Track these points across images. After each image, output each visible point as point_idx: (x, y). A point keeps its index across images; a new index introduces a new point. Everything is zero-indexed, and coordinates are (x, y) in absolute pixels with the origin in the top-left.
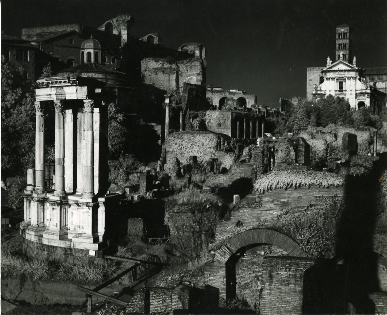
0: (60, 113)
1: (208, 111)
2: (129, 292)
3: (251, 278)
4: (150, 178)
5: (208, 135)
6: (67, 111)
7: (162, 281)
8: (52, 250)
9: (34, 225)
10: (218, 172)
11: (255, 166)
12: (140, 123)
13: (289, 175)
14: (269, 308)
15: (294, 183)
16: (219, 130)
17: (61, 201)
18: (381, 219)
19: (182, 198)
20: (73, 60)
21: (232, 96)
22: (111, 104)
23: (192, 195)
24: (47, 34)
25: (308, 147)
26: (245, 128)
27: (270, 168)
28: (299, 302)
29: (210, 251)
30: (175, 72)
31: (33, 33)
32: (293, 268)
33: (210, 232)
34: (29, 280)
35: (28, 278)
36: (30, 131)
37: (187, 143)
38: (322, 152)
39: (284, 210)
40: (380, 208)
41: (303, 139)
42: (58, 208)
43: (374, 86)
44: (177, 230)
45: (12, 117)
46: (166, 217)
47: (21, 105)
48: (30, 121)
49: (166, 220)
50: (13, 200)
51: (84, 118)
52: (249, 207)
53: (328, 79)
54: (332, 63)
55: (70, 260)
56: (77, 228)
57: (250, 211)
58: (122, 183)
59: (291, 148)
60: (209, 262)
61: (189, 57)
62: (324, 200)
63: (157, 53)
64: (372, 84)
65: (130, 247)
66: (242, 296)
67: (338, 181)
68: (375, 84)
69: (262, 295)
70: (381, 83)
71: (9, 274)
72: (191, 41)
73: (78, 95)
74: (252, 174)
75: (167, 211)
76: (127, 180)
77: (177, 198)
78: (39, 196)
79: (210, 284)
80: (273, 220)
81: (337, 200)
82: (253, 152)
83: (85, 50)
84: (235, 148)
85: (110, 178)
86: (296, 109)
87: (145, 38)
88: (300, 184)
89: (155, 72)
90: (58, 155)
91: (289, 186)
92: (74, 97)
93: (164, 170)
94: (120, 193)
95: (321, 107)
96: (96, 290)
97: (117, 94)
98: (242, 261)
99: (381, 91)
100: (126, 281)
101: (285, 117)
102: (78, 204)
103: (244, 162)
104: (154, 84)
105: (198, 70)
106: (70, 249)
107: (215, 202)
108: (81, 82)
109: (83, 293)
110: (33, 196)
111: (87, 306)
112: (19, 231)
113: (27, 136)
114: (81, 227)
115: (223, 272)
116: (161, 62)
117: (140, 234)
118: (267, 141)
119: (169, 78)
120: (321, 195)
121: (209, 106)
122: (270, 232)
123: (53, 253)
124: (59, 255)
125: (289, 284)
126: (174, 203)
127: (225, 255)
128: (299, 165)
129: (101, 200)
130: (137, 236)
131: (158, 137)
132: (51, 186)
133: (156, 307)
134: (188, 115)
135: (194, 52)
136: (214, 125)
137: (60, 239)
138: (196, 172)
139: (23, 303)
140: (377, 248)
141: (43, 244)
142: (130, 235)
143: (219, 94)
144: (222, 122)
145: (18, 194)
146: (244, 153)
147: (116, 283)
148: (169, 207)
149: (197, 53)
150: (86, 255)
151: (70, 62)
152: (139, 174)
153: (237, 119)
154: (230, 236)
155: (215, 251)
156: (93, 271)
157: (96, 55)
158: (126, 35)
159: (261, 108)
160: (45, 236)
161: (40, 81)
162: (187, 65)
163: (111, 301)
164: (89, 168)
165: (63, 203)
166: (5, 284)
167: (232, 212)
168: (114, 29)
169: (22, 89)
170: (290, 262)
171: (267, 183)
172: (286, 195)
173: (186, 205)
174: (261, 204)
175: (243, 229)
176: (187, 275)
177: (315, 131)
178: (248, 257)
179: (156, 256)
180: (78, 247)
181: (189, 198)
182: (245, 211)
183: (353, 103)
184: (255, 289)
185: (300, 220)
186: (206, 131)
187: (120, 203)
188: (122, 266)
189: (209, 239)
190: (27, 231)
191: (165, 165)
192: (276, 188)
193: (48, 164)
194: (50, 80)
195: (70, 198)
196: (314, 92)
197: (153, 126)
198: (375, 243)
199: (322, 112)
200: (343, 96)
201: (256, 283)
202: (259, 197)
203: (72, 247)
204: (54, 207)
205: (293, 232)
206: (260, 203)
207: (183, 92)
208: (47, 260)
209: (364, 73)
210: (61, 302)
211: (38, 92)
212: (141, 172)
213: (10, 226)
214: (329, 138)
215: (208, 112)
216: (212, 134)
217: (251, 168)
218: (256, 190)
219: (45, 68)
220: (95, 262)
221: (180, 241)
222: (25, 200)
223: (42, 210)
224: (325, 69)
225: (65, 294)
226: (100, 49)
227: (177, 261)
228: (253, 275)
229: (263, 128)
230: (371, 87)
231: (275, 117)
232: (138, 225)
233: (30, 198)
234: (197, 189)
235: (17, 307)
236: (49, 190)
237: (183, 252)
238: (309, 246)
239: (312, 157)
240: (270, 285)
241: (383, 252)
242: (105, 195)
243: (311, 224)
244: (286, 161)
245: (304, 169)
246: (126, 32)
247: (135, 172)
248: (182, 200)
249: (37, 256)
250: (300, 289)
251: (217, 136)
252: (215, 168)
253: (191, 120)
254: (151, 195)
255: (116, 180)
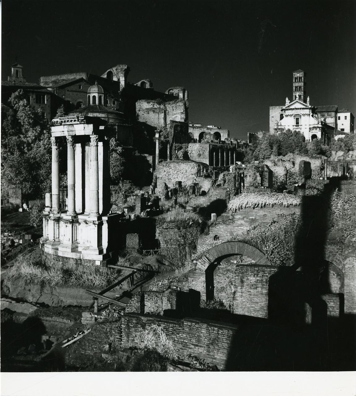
0: (72, 147)
1: (190, 144)
2: (127, 295)
3: (227, 283)
4: (144, 200)
5: (190, 163)
6: (77, 145)
7: (154, 285)
8: (66, 261)
9: (51, 240)
10: (198, 194)
11: (228, 189)
12: (136, 154)
13: (256, 196)
14: (241, 308)
15: (260, 203)
16: (199, 159)
17: (73, 220)
18: (331, 232)
19: (169, 216)
20: (81, 102)
21: (209, 131)
22: (112, 138)
23: (178, 214)
24: (60, 81)
25: (271, 173)
26: (221, 158)
27: (241, 190)
28: (265, 302)
29: (193, 260)
30: (163, 111)
31: (49, 80)
32: (260, 274)
33: (193, 244)
34: (47, 285)
35: (47, 284)
36: (47, 162)
37: (173, 171)
38: (282, 177)
39: (253, 226)
40: (330, 223)
41: (267, 166)
42: (70, 226)
43: (324, 121)
44: (166, 244)
45: (33, 150)
46: (157, 232)
47: (40, 140)
48: (48, 154)
49: (157, 235)
50: (34, 219)
51: (91, 150)
52: (224, 223)
53: (287, 116)
54: (290, 103)
55: (80, 269)
56: (85, 242)
57: (225, 227)
58: (121, 205)
59: (258, 174)
60: (192, 269)
61: (174, 98)
62: (285, 217)
63: (149, 96)
64: (322, 119)
65: (128, 258)
66: (219, 298)
67: (296, 201)
68: (325, 120)
69: (235, 297)
70: (330, 119)
71: (32, 281)
72: (176, 85)
73: (86, 131)
74: (226, 196)
75: (158, 228)
76: (126, 202)
77: (166, 217)
78: (55, 216)
79: (193, 288)
80: (244, 234)
81: (295, 217)
82: (227, 178)
83: (91, 94)
84: (212, 174)
85: (112, 200)
86: (261, 142)
87: (139, 84)
88: (265, 204)
89: (147, 112)
90: (70, 182)
91: (256, 206)
92: (82, 133)
93: (155, 193)
94: (120, 213)
95: (281, 139)
96: (101, 294)
97: (117, 130)
98: (219, 269)
99: (330, 125)
100: (125, 286)
101: (252, 148)
102: (86, 222)
103: (219, 185)
104: (147, 122)
105: (182, 109)
106: (80, 260)
107: (196, 219)
108: (88, 121)
109: (91, 296)
110: (50, 216)
111: (94, 307)
112: (39, 245)
113: (45, 166)
114: (89, 241)
115: (203, 278)
116: (152, 103)
117: (136, 247)
118: (238, 168)
119: (159, 116)
120: (282, 213)
121: (191, 140)
122: (241, 244)
123: (67, 263)
124: (71, 265)
125: (257, 288)
126: (163, 221)
127: (205, 263)
128: (264, 188)
129: (105, 219)
130: (134, 248)
131: (150, 166)
132: (64, 207)
133: (149, 308)
134: (174, 147)
135: (178, 94)
136: (195, 155)
137: (72, 252)
138: (181, 194)
139: (43, 305)
140: (329, 257)
141: (59, 256)
142: (128, 248)
143: (199, 129)
144: (201, 153)
145: (38, 215)
146: (220, 179)
147: (118, 287)
148: (159, 224)
149: (181, 95)
150: (93, 264)
151: (79, 104)
152: (135, 197)
153: (213, 150)
154: (209, 248)
155: (197, 260)
156: (99, 278)
157: (100, 98)
158: (124, 81)
159: (233, 141)
160: (60, 248)
161: (54, 120)
162: (173, 105)
163: (113, 302)
164: (95, 192)
165: (74, 221)
166: (28, 289)
167: (210, 228)
168: (114, 77)
169: (40, 127)
170: (257, 269)
171: (239, 204)
172: (254, 213)
173: (173, 222)
174: (234, 221)
175: (219, 242)
176: (174, 281)
177: (276, 160)
178: (223, 265)
179: (149, 265)
180: (86, 258)
181: (175, 216)
182: (221, 227)
183: (308, 136)
184: (229, 292)
185: (266, 234)
186: (188, 160)
187: (120, 221)
188: (122, 274)
189: (192, 251)
190: (45, 245)
191: (156, 189)
192: (245, 207)
193: (62, 189)
194: (63, 119)
195: (80, 217)
196: (276, 127)
197: (145, 157)
198: (326, 253)
199: (282, 143)
200: (300, 130)
201: (230, 287)
202: (232, 215)
203: (81, 258)
204: (67, 225)
205: (260, 244)
206: (233, 220)
207: (170, 128)
208: (62, 269)
209: (316, 111)
210: (73, 304)
211: (53, 129)
212: (136, 195)
213: (32, 241)
214: (289, 165)
215: (190, 145)
216: (193, 163)
217: (225, 191)
218: (229, 209)
219: (59, 110)
220: (101, 270)
221: (169, 252)
222: (44, 219)
223: (58, 227)
224: (284, 108)
225: (77, 297)
226: (103, 93)
227: (166, 269)
228: (228, 280)
229: (234, 157)
230: (322, 122)
231: (244, 148)
232: (134, 239)
233: (47, 217)
234: (182, 209)
235: (38, 308)
236: (63, 210)
237: (171, 262)
238: (273, 256)
239: (274, 181)
240: (241, 289)
241: (333, 260)
242: (108, 215)
243: (274, 238)
244: (253, 185)
245: (268, 191)
246: (124, 79)
247: (131, 195)
248: (169, 218)
249: (54, 266)
250: (266, 291)
251: (198, 164)
252: (196, 191)
253: (177, 151)
254: (145, 215)
255: (116, 202)
